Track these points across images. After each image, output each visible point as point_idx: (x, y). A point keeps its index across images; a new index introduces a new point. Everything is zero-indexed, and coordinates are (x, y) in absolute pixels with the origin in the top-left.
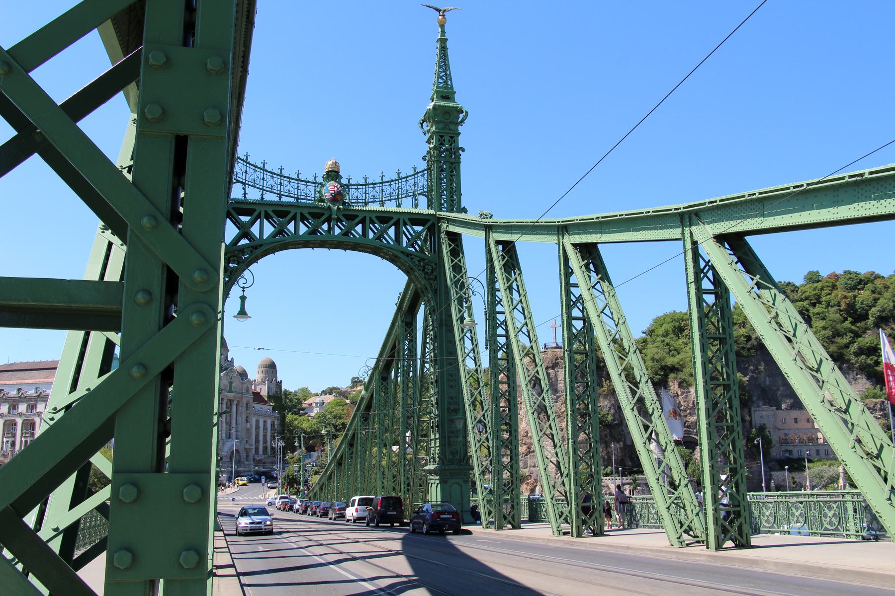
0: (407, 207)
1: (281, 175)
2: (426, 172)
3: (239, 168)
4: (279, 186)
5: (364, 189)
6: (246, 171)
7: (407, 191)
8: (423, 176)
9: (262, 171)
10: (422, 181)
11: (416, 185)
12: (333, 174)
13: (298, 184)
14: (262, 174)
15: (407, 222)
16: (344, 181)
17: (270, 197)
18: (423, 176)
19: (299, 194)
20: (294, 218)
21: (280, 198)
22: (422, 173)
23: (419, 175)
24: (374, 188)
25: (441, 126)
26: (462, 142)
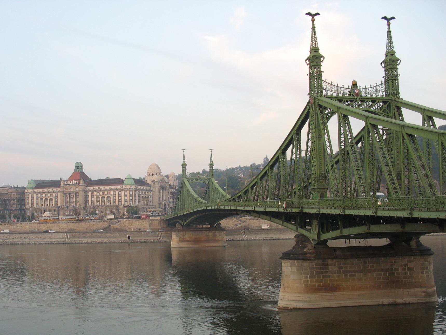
0: (380, 95)
1: (338, 86)
3: (324, 84)
6: (326, 86)
12: (354, 84)
16: (359, 88)
17: (335, 94)
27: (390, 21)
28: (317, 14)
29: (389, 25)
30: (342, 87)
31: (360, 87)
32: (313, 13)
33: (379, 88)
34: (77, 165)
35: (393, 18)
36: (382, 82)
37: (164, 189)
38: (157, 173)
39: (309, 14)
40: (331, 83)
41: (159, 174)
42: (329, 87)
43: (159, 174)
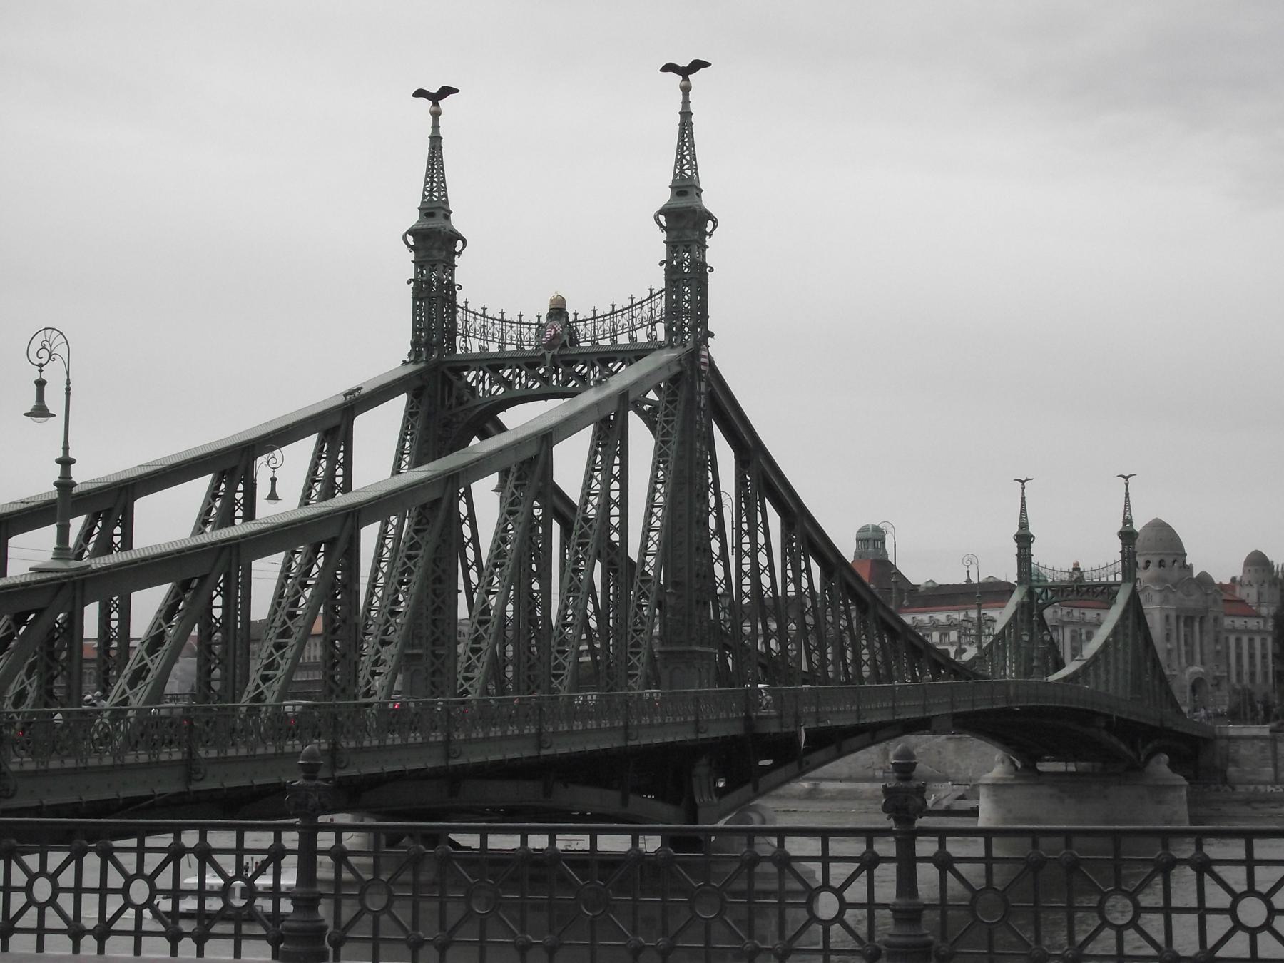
0: (642, 336)
1: (502, 320)
3: (460, 316)
5: (593, 324)
7: (642, 319)
11: (653, 311)
12: (558, 311)
13: (521, 327)
15: (634, 360)
16: (571, 318)
17: (493, 348)
18: (661, 298)
23: (657, 297)
24: (604, 321)
25: (674, 233)
27: (690, 76)
28: (446, 91)
29: (686, 90)
31: (576, 314)
32: (434, 89)
33: (643, 313)
34: (865, 535)
35: (698, 65)
36: (651, 290)
37: (1198, 619)
38: (1162, 557)
39: (420, 93)
40: (481, 312)
41: (1175, 561)
42: (476, 325)
43: (1175, 561)
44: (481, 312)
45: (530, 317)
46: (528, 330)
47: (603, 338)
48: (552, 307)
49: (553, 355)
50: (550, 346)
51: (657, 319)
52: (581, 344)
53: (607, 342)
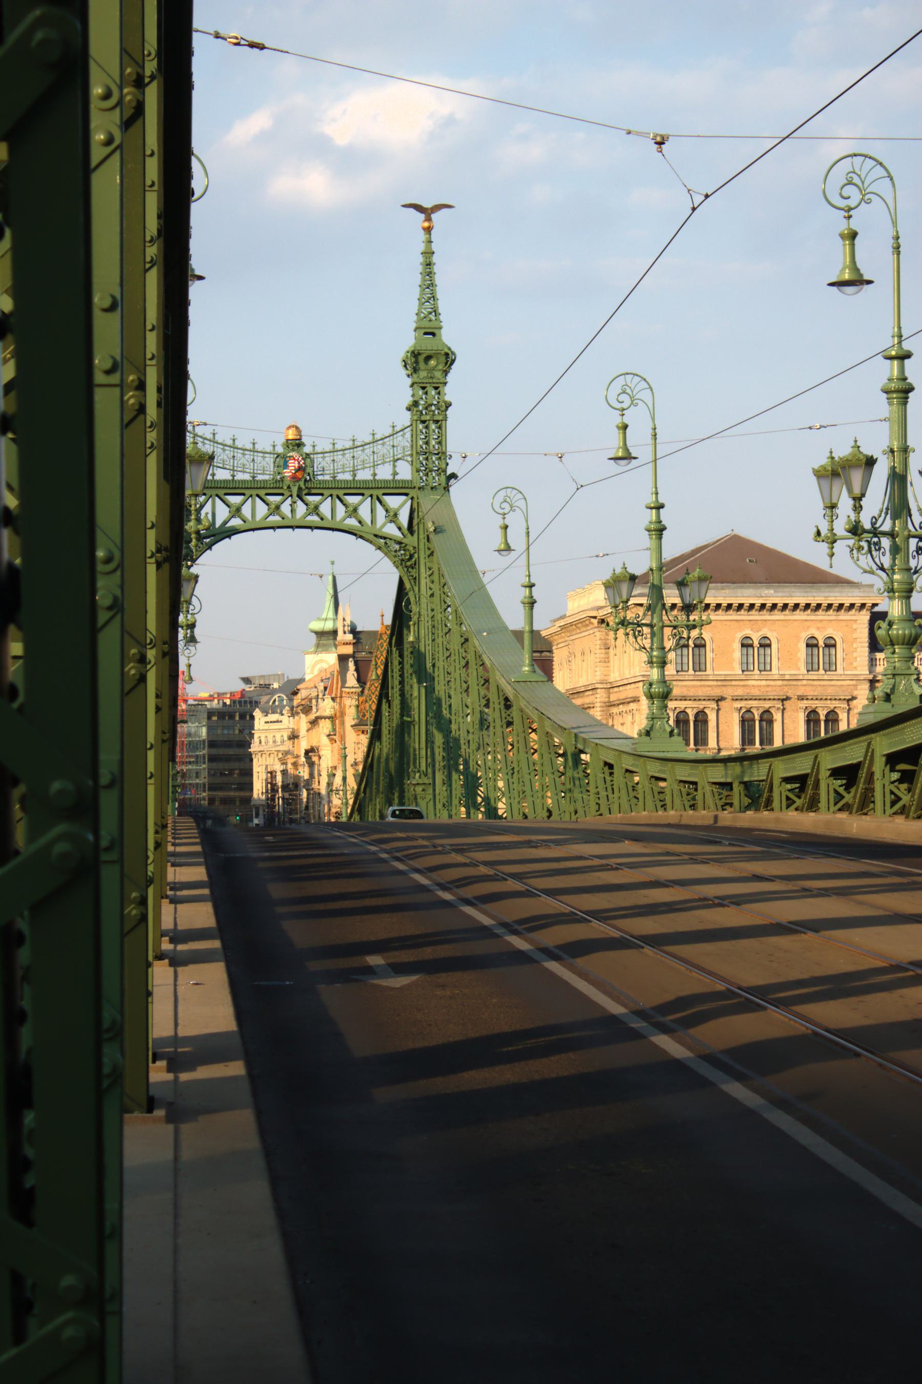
0: (385, 473)
1: (234, 447)
2: (409, 429)
4: (232, 460)
8: (403, 436)
9: (212, 443)
10: (404, 441)
14: (212, 447)
16: (307, 449)
18: (403, 436)
19: (256, 468)
20: (251, 496)
21: (233, 476)
22: (402, 433)
24: (344, 455)
26: (449, 393)
27: (433, 216)
30: (249, 446)
40: (211, 437)
44: (211, 437)
45: (264, 445)
46: (221, 451)
47: (343, 472)
48: (290, 437)
49: (300, 489)
50: (294, 478)
51: (399, 456)
52: (320, 478)
53: (348, 477)
